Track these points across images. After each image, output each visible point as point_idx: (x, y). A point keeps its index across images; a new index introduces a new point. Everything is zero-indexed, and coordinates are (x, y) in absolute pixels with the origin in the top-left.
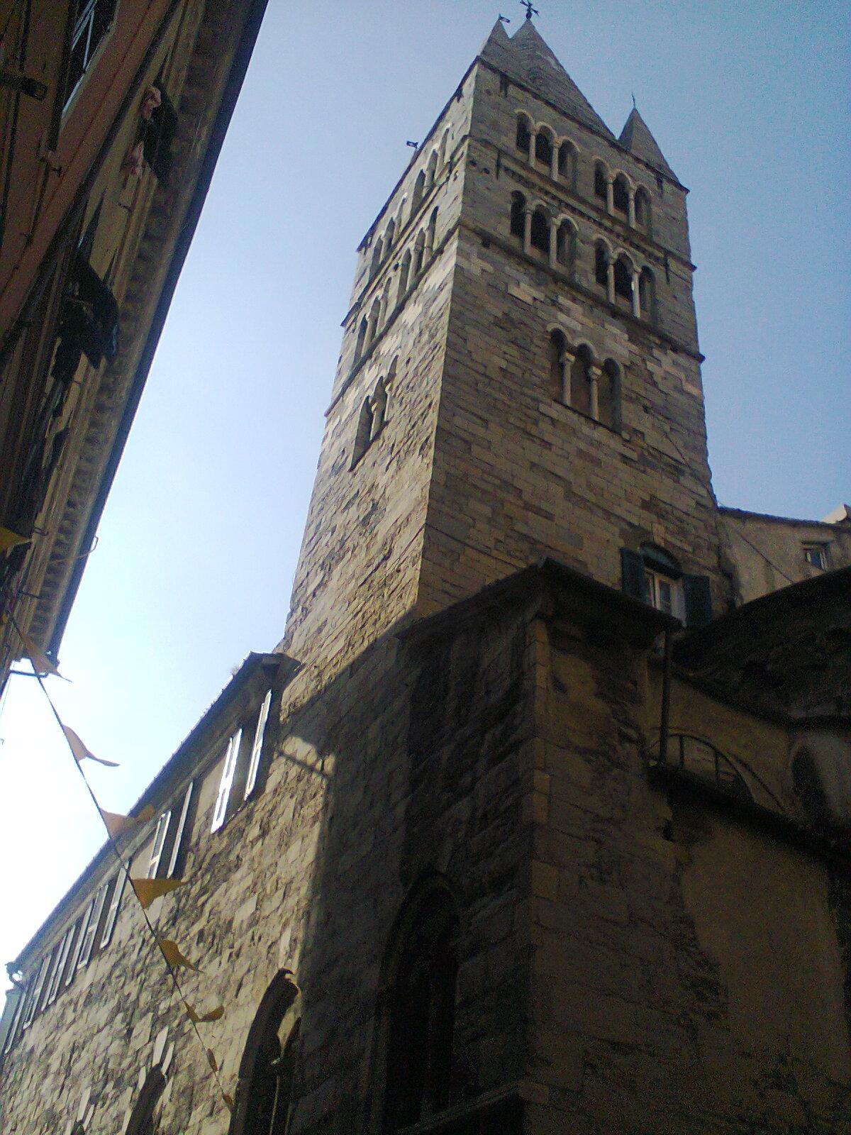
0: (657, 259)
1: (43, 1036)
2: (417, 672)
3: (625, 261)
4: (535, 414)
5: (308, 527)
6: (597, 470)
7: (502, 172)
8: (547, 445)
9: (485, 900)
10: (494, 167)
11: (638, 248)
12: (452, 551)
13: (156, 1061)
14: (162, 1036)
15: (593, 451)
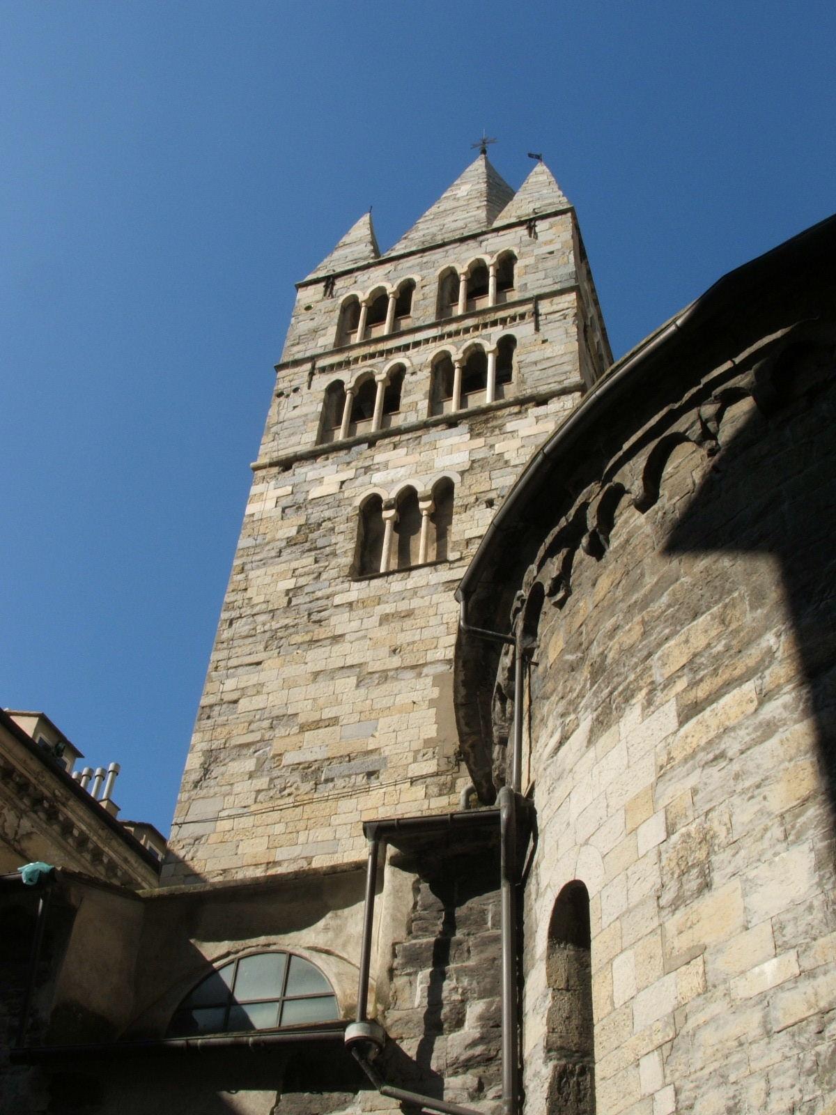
0: (522, 316)
6: (408, 623)
8: (337, 639)
15: (403, 606)
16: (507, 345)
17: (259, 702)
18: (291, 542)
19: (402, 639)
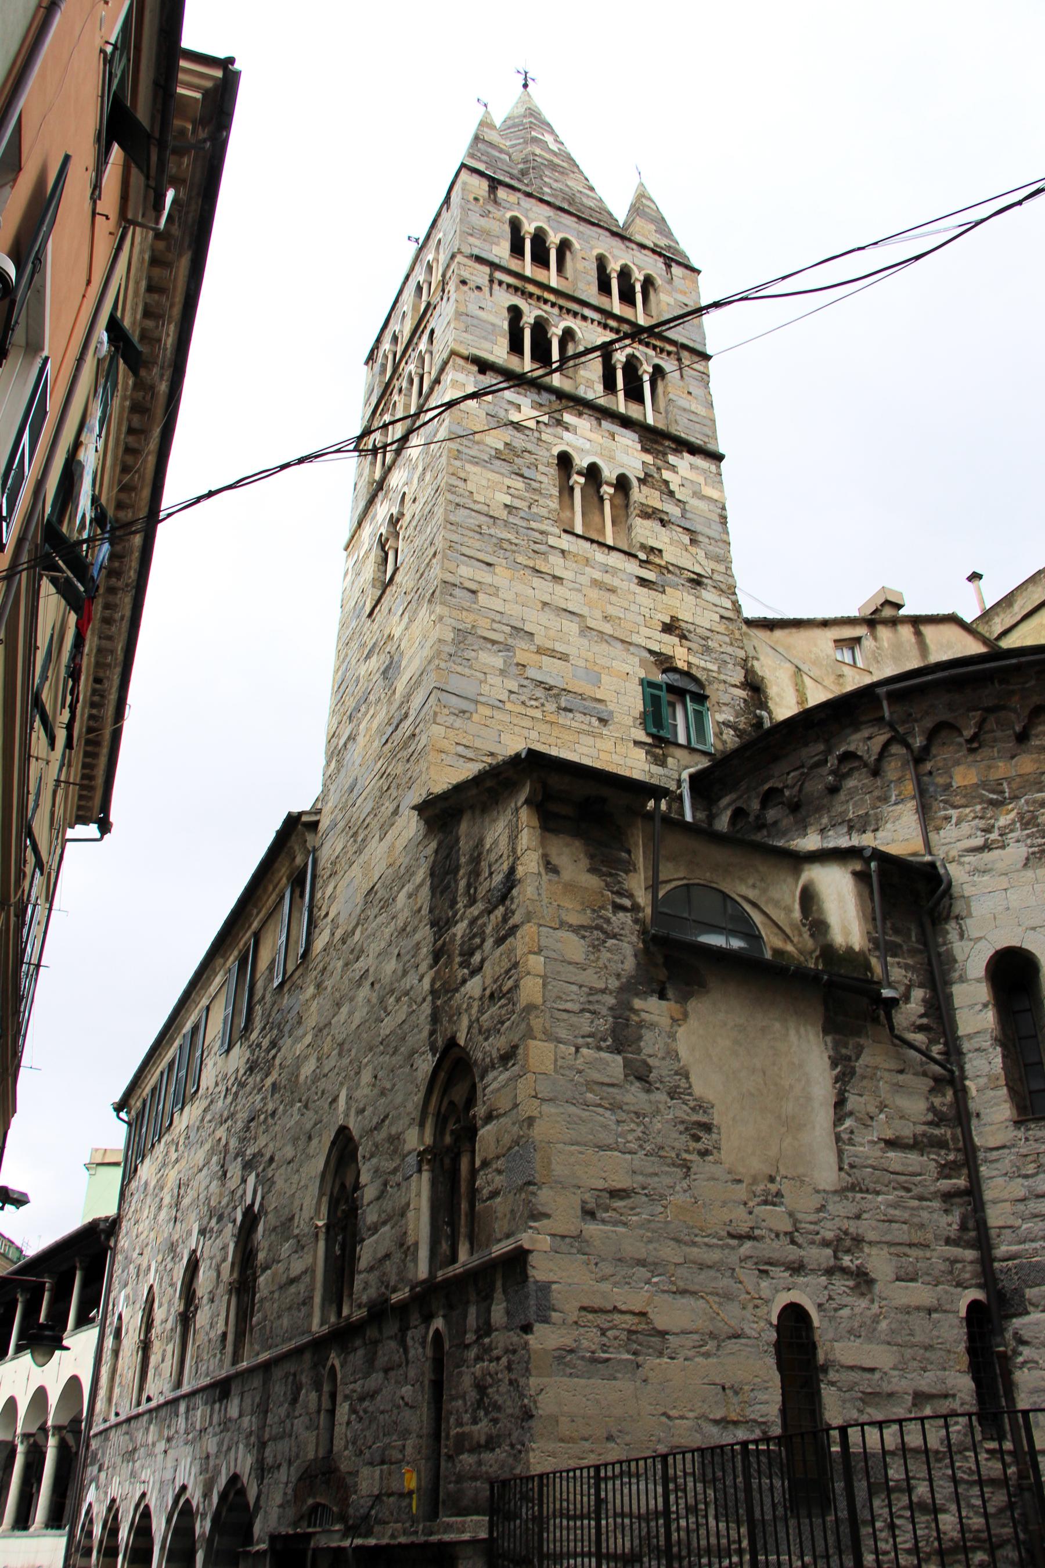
0: (669, 353)
1: (153, 1170)
2: (434, 845)
3: (635, 361)
4: (542, 548)
5: (337, 671)
6: (613, 598)
7: (496, 286)
8: (558, 579)
9: (495, 1073)
10: (487, 283)
11: (647, 345)
12: (464, 712)
13: (249, 1201)
14: (251, 1179)
15: (607, 579)
17: (496, 604)
18: (498, 456)
19: (611, 610)
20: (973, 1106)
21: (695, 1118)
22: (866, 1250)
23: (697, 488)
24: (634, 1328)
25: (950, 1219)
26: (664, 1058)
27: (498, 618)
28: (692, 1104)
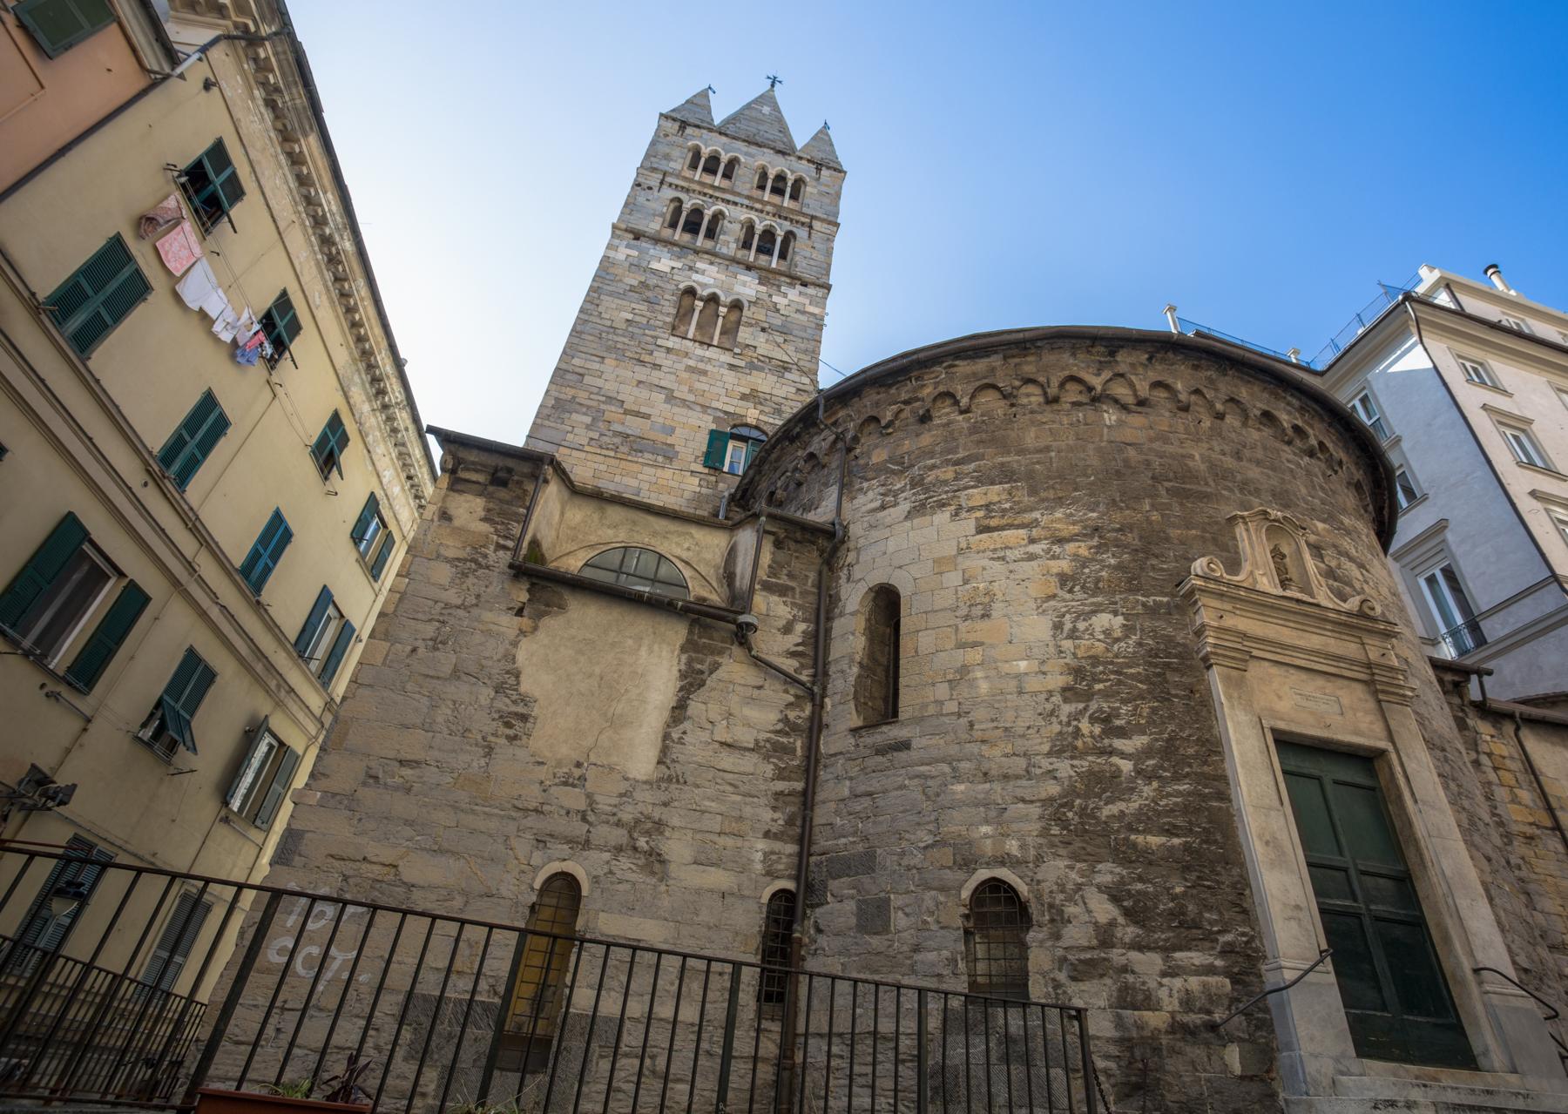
0: (803, 224)
6: (703, 378)
8: (657, 367)
15: (701, 366)
16: (789, 236)
17: (599, 382)
18: (632, 289)
19: (698, 385)
20: (825, 719)
21: (514, 709)
22: (667, 834)
23: (800, 308)
24: (380, 878)
25: (776, 816)
26: (499, 661)
27: (596, 390)
28: (514, 698)
